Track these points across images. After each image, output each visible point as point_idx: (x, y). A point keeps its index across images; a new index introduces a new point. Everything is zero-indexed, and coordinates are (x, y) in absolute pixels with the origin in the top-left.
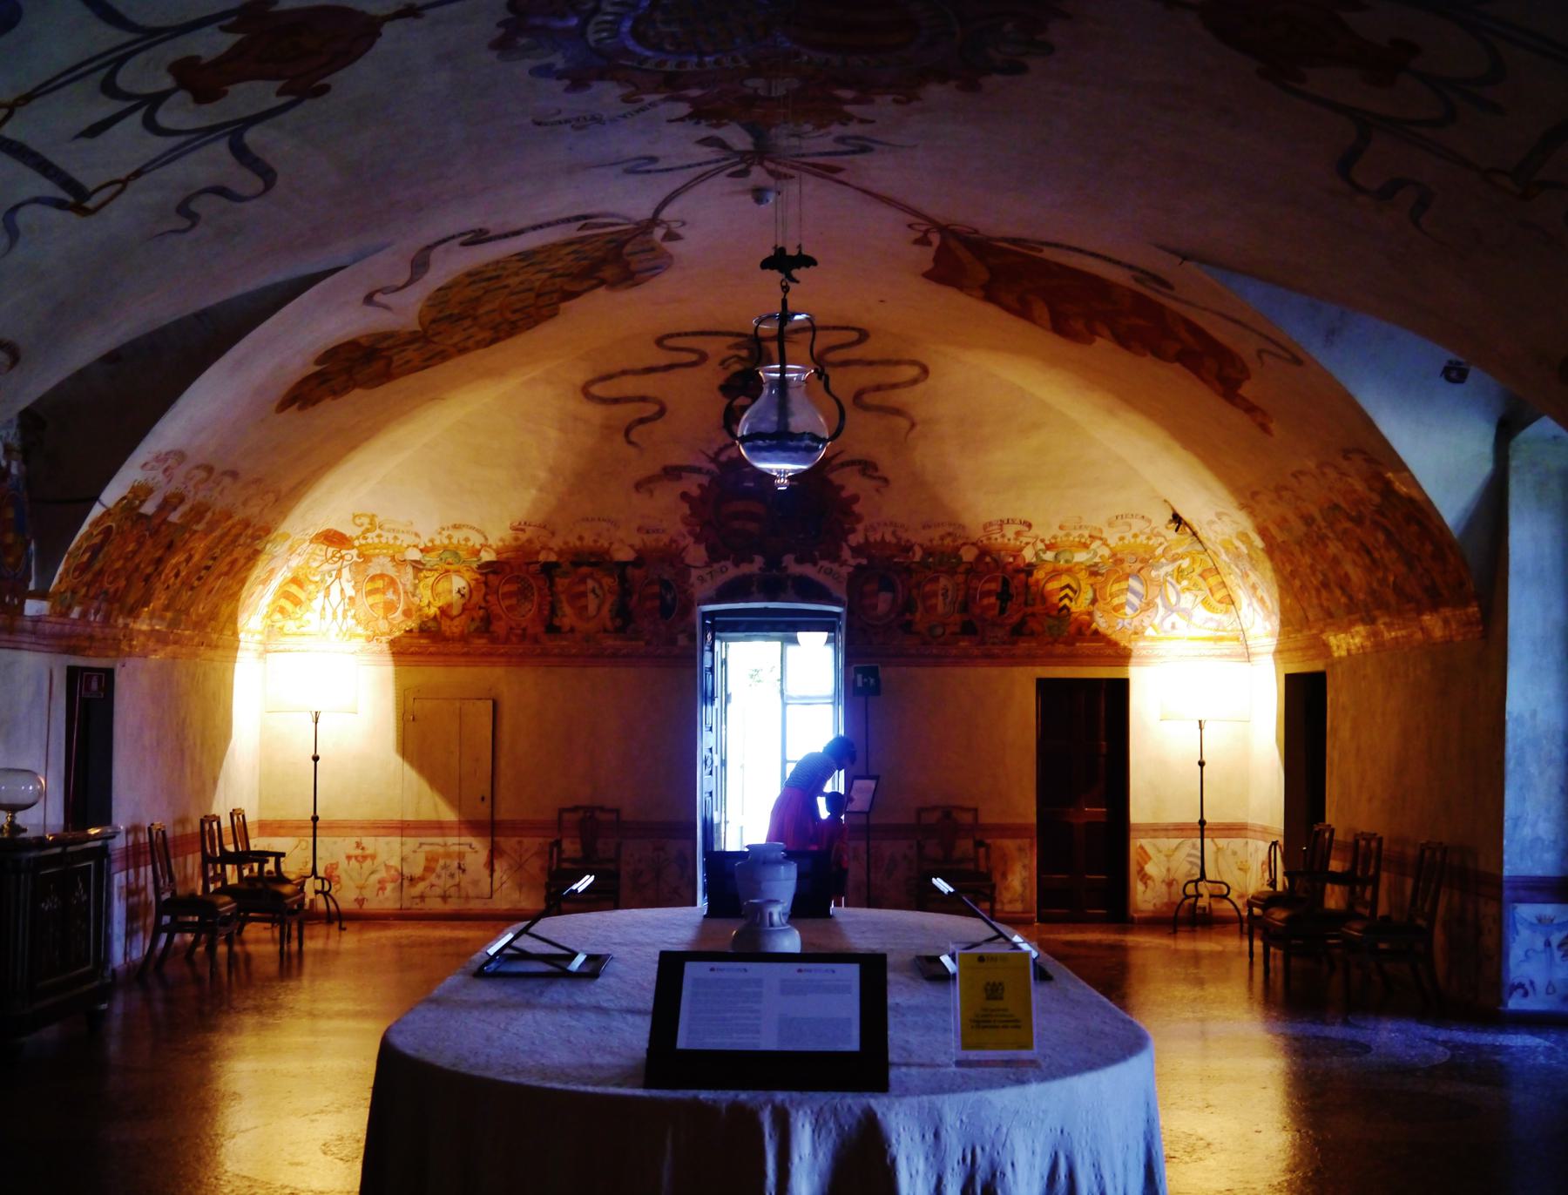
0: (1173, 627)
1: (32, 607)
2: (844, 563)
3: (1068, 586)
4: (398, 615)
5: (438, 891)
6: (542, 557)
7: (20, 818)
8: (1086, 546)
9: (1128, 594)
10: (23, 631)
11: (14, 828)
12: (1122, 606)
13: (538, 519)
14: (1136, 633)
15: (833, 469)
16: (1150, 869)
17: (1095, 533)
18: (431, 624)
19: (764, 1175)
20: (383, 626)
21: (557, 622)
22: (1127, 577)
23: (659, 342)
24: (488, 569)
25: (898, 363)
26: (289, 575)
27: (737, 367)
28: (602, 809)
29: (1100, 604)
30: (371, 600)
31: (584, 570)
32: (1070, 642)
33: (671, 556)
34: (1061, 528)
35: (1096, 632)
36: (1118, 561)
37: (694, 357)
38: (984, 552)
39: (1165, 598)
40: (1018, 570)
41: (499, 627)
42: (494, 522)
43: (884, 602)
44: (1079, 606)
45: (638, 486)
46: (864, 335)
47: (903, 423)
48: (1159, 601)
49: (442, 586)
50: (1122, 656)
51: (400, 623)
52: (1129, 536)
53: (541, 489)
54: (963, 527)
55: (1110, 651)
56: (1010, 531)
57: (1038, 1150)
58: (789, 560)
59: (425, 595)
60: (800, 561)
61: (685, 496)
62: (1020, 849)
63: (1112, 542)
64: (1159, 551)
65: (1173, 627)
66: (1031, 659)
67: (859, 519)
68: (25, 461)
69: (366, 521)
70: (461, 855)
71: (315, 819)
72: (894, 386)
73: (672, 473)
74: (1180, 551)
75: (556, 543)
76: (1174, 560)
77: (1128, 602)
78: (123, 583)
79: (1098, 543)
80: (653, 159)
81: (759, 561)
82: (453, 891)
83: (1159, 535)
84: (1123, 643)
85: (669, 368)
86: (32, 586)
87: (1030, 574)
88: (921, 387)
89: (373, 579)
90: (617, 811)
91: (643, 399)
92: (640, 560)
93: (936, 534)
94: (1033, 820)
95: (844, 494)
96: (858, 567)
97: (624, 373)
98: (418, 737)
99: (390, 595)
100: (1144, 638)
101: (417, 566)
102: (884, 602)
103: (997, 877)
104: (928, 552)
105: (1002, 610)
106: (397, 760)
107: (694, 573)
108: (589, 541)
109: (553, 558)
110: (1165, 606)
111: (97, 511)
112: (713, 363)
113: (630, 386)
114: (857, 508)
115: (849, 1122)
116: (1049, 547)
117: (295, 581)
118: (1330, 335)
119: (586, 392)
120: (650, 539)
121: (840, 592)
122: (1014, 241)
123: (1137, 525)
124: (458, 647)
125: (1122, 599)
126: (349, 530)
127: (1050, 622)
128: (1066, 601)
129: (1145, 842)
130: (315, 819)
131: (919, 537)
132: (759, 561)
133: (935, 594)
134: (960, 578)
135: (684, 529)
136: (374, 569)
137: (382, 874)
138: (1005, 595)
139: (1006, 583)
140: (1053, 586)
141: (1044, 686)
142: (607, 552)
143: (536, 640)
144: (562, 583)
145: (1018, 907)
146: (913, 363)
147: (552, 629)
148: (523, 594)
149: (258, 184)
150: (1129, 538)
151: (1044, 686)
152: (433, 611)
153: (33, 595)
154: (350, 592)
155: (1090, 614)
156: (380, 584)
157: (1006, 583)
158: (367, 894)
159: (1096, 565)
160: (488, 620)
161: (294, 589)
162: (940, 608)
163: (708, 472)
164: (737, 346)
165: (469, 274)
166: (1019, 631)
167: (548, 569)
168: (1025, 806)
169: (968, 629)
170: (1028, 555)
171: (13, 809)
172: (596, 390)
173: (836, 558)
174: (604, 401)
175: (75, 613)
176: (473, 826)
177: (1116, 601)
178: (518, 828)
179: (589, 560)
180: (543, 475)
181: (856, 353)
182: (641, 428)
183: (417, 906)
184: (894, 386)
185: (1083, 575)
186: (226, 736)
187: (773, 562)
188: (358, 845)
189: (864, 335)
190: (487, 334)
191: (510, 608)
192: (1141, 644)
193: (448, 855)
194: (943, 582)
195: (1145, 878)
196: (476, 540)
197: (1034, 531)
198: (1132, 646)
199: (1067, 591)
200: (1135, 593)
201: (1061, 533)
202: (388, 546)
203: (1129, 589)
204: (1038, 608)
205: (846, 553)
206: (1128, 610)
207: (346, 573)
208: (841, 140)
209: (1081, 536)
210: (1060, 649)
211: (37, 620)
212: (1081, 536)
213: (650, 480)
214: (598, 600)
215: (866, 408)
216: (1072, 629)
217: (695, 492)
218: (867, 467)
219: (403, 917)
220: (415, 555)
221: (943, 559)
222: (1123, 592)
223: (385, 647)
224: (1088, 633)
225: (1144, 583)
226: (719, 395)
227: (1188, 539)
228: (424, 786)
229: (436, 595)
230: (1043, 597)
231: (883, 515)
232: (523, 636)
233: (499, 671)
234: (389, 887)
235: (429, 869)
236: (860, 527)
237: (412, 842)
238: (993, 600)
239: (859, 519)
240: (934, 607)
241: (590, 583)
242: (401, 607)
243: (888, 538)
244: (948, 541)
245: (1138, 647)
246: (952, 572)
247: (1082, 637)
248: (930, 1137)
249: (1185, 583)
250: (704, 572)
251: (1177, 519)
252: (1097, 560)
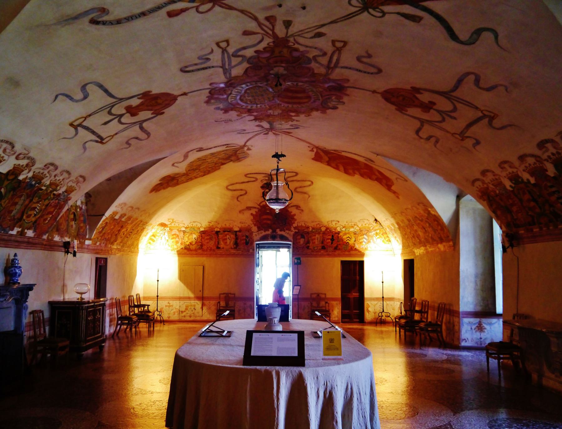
1: (87, 242)
2: (292, 231)
4: (179, 244)
5: (189, 315)
6: (216, 230)
7: (84, 296)
8: (353, 227)
9: (364, 239)
10: (85, 248)
11: (82, 299)
12: (362, 242)
13: (215, 220)
15: (289, 207)
16: (370, 309)
18: (188, 247)
19: (273, 388)
20: (175, 247)
21: (219, 246)
22: (363, 235)
23: (246, 175)
24: (203, 233)
25: (305, 181)
26: (152, 234)
27: (265, 182)
28: (230, 294)
29: (357, 242)
30: (172, 240)
31: (226, 233)
32: (349, 251)
33: (249, 230)
35: (356, 249)
37: (254, 179)
38: (327, 228)
39: (373, 240)
40: (336, 233)
41: (205, 247)
42: (204, 222)
43: (302, 241)
44: (351, 242)
45: (240, 212)
46: (297, 174)
47: (306, 196)
49: (190, 237)
50: (362, 255)
51: (179, 246)
53: (215, 212)
54: (322, 222)
56: (334, 223)
57: (343, 381)
58: (278, 230)
59: (186, 239)
60: (281, 231)
61: (252, 214)
62: (337, 304)
63: (360, 226)
66: (339, 256)
67: (295, 220)
68: (86, 205)
69: (171, 220)
70: (194, 306)
71: (158, 296)
72: (305, 187)
73: (249, 208)
75: (219, 226)
76: (375, 230)
78: (110, 236)
80: (245, 130)
81: (270, 231)
82: (192, 315)
85: (248, 182)
86: (87, 237)
87: (339, 234)
88: (311, 187)
89: (173, 235)
90: (234, 294)
91: (241, 190)
92: (240, 231)
93: (315, 224)
94: (340, 296)
95: (292, 214)
96: (296, 232)
97: (237, 183)
98: (184, 276)
99: (177, 239)
101: (184, 232)
102: (302, 241)
103: (331, 311)
104: (313, 229)
105: (332, 243)
106: (178, 281)
107: (254, 234)
108: (228, 225)
109: (218, 230)
111: (104, 218)
112: (259, 181)
113: (238, 187)
114: (295, 217)
115: (295, 375)
116: (344, 227)
117: (153, 236)
118: (414, 174)
119: (227, 188)
120: (243, 225)
121: (291, 238)
122: (335, 151)
123: (366, 222)
124: (194, 253)
125: (362, 240)
126: (167, 223)
127: (344, 246)
129: (368, 302)
130: (158, 296)
131: (311, 225)
132: (270, 231)
133: (315, 239)
134: (321, 235)
135: (251, 222)
136: (173, 233)
137: (175, 310)
138: (332, 240)
139: (333, 236)
140: (345, 237)
141: (343, 262)
142: (232, 228)
143: (214, 251)
144: (220, 236)
145: (336, 319)
146: (309, 181)
147: (218, 248)
148: (211, 239)
149: (146, 136)
150: (364, 225)
151: (343, 262)
152: (188, 243)
153: (88, 239)
154: (167, 238)
156: (174, 236)
157: (333, 236)
158: (170, 315)
160: (202, 245)
161: (153, 238)
162: (316, 243)
163: (258, 208)
164: (265, 177)
165: (198, 159)
166: (336, 248)
167: (217, 233)
168: (337, 292)
169: (323, 248)
170: (338, 229)
171: (82, 294)
172: (230, 187)
173: (289, 230)
174: (231, 190)
175: (98, 244)
176: (198, 298)
177: (361, 241)
178: (209, 299)
179: (228, 230)
180: (216, 209)
181: (295, 178)
182: (241, 197)
183: (184, 319)
184: (305, 187)
185: (352, 234)
186: (135, 276)
187: (274, 231)
188: (168, 303)
189: (297, 174)
190: (202, 174)
191: (208, 243)
193: (191, 305)
194: (317, 236)
195: (368, 311)
196: (199, 225)
197: (340, 223)
202: (177, 227)
204: (341, 242)
205: (292, 229)
206: (364, 243)
207: (166, 234)
208: (292, 125)
210: (347, 253)
211: (88, 245)
213: (243, 210)
214: (230, 240)
215: (298, 192)
216: (350, 248)
217: (254, 213)
218: (298, 207)
219: (180, 321)
220: (184, 229)
221: (317, 230)
222: (362, 238)
223: (176, 252)
225: (368, 236)
226: (260, 189)
227: (379, 225)
228: (185, 288)
229: (189, 239)
230: (342, 240)
231: (302, 219)
232: (211, 250)
233: (204, 258)
234: (176, 313)
235: (186, 309)
236: (296, 222)
237: (182, 302)
238: (329, 240)
239: (295, 220)
240: (315, 242)
241: (228, 236)
242: (180, 242)
243: (303, 225)
244: (318, 226)
245: (366, 253)
246: (319, 233)
247: (352, 250)
248: (316, 378)
249: (378, 236)
250: (256, 233)
251: (376, 220)
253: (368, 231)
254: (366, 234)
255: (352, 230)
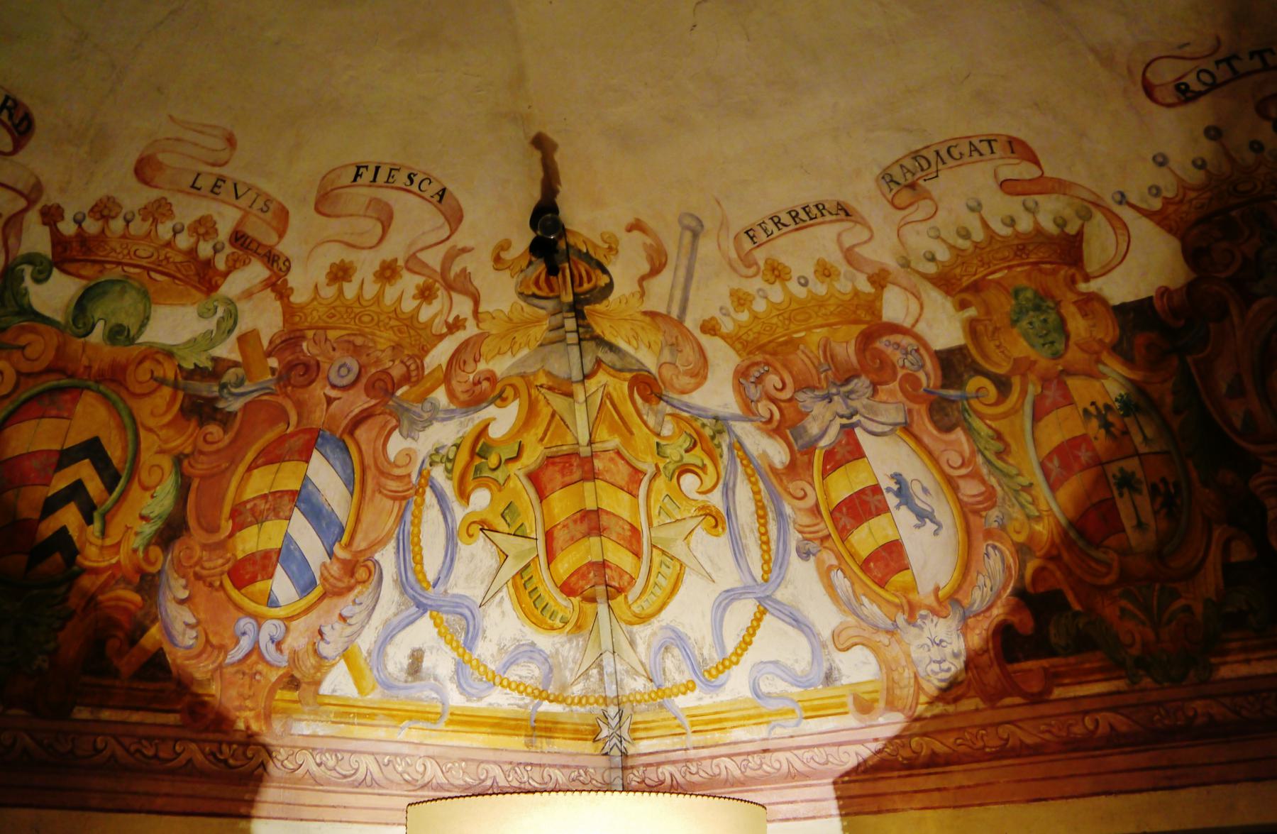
0: (415, 666)
3: (92, 450)
8: (204, 278)
9: (300, 509)
12: (262, 564)
14: (292, 683)
17: (260, 231)
22: (306, 444)
29: (194, 543)
34: (144, 170)
35: (157, 664)
36: (298, 371)
39: (409, 550)
44: (114, 542)
48: (386, 558)
52: (366, 264)
55: (194, 752)
63: (305, 280)
64: (439, 355)
65: (415, 666)
74: (501, 366)
76: (475, 401)
77: (287, 554)
79: (256, 272)
83: (463, 285)
84: (246, 719)
100: (318, 705)
110: (403, 585)
116: (67, 253)
123: (415, 220)
128: (70, 517)
155: (148, 584)
159: (216, 370)
177: (250, 541)
185: (156, 409)
192: (304, 728)
198: (273, 733)
199: (85, 471)
200: (318, 515)
201: (135, 197)
203: (303, 499)
206: (282, 585)
209: (204, 227)
212: (204, 227)
224: (127, 664)
225: (359, 480)
252: (227, 350)
253: (382, 387)
254: (339, 440)
255: (175, 325)
